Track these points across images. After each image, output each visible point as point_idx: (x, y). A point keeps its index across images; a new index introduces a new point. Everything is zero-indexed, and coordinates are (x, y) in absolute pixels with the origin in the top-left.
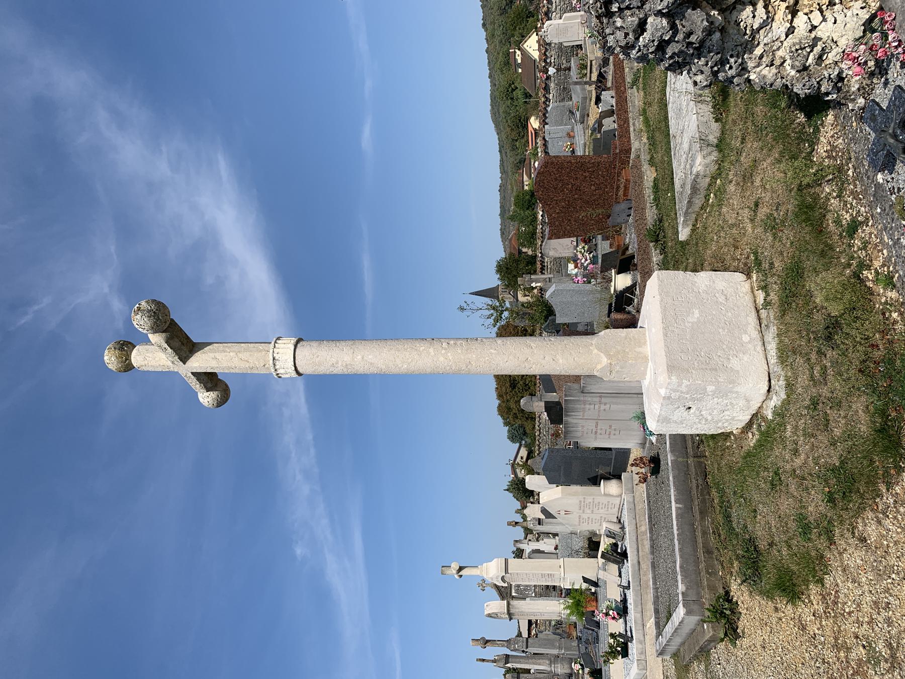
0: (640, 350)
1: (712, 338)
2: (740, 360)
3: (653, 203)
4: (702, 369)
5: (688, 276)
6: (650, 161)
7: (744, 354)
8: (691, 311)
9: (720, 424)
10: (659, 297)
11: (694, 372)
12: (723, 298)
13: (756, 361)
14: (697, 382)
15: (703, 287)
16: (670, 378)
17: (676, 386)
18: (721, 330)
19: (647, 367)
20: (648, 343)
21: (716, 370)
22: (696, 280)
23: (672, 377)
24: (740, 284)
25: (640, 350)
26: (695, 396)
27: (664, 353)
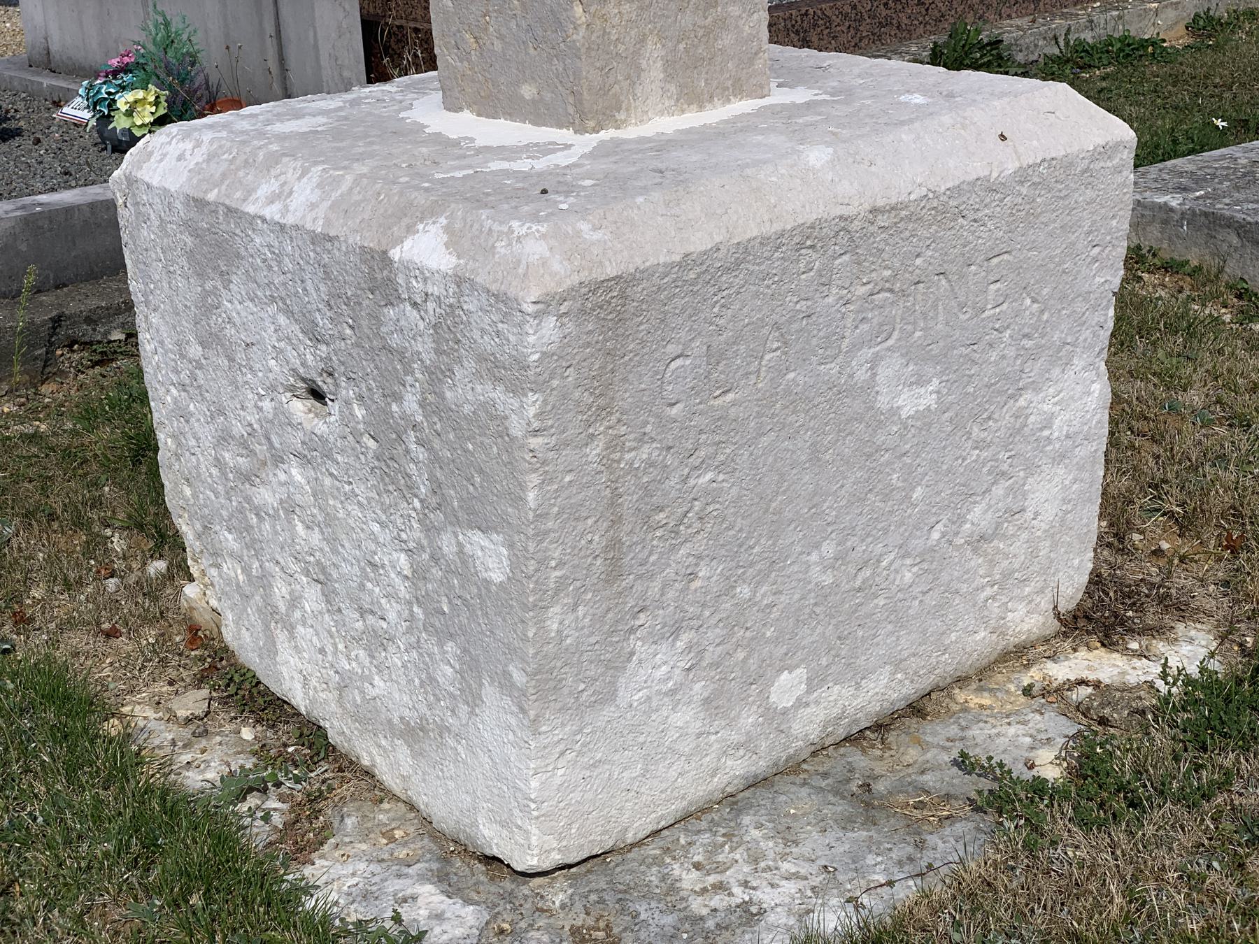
0: (654, 72)
1: (788, 515)
2: (673, 692)
3: (1067, 44)
4: (616, 494)
5: (1097, 318)
6: (1210, 19)
7: (707, 701)
8: (929, 370)
9: (229, 540)
10: (1011, 167)
11: (595, 451)
12: (986, 524)
13: (673, 774)
14: (534, 479)
15: (1040, 404)
16: (546, 305)
17: (488, 344)
18: (828, 549)
19: (538, 121)
20: (693, 119)
21: (614, 572)
22: (1078, 363)
23: (551, 321)
24: (1041, 591)
25: (654, 72)
26: (421, 454)
27: (699, 242)
